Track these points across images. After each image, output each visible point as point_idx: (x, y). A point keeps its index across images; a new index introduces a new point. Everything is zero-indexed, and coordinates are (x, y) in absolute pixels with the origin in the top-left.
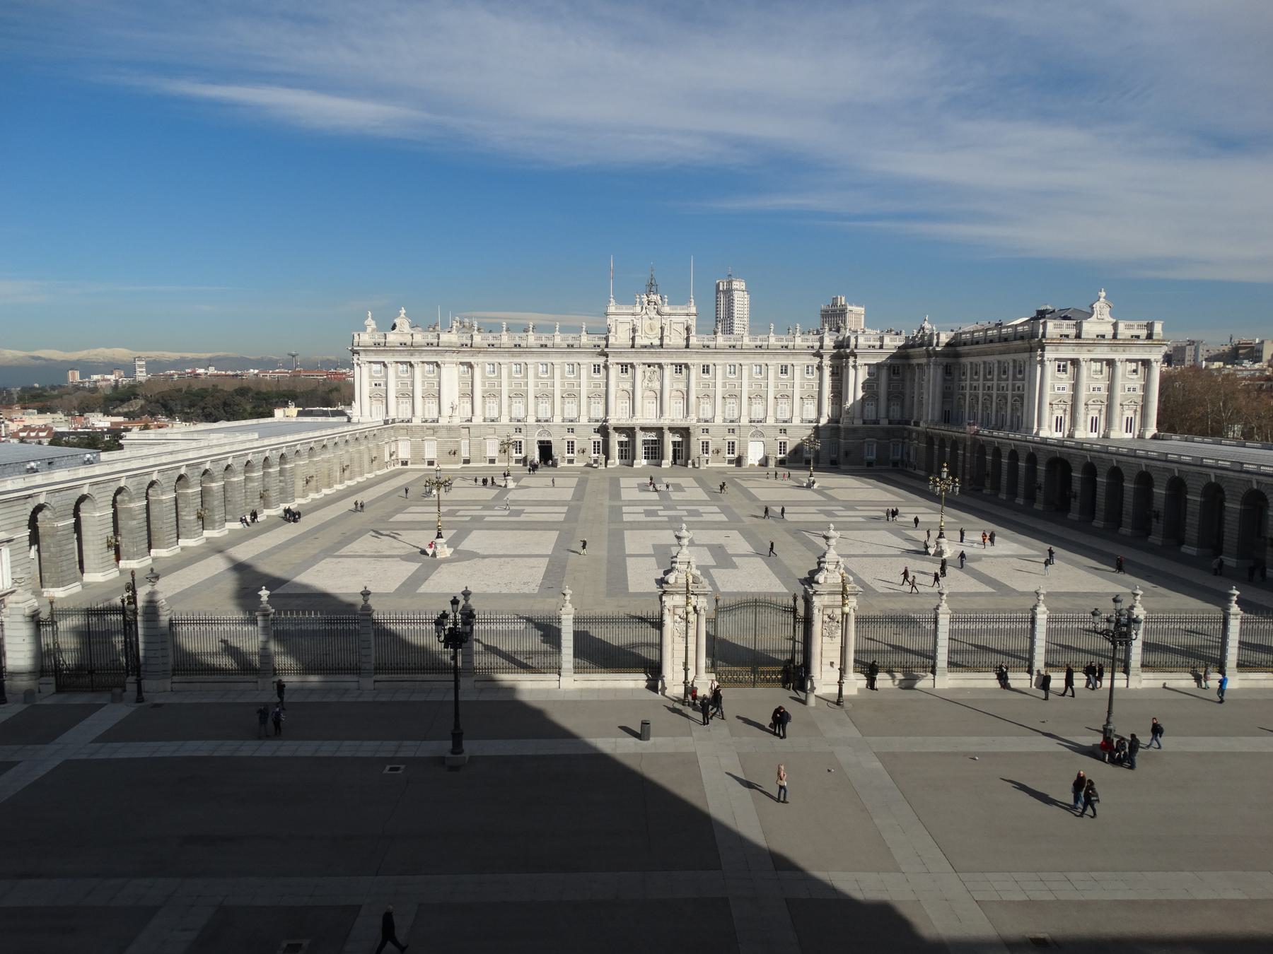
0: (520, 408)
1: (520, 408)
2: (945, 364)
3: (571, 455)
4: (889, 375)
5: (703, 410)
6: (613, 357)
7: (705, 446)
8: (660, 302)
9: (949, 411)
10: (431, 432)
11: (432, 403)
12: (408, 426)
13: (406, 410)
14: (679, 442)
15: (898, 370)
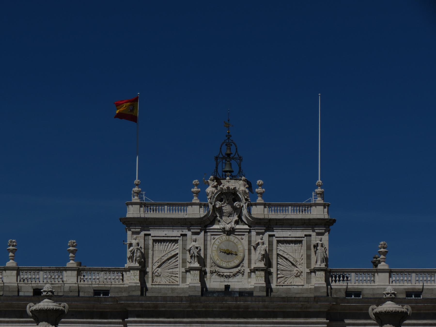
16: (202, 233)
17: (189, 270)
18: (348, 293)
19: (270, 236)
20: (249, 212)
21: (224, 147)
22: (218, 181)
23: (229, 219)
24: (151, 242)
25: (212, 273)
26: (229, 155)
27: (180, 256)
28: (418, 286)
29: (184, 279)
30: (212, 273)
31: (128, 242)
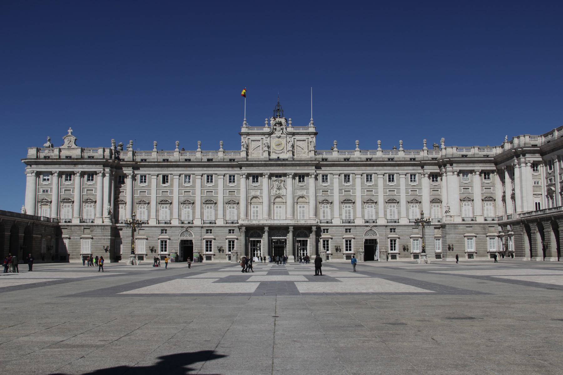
0: (166, 212)
1: (166, 212)
2: (532, 162)
3: (209, 253)
4: (482, 179)
5: (324, 213)
6: (246, 168)
7: (326, 242)
8: (285, 124)
9: (539, 203)
10: (88, 231)
11: (91, 207)
12: (68, 226)
13: (68, 212)
14: (303, 241)
15: (489, 176)
16: (269, 137)
17: (264, 151)
18: (323, 160)
19: (294, 139)
20: (286, 129)
21: (277, 107)
22: (274, 118)
23: (279, 133)
24: (250, 141)
25: (273, 152)
26: (278, 110)
27: (261, 146)
28: (348, 156)
29: (262, 155)
30: (273, 152)
31: (242, 141)
